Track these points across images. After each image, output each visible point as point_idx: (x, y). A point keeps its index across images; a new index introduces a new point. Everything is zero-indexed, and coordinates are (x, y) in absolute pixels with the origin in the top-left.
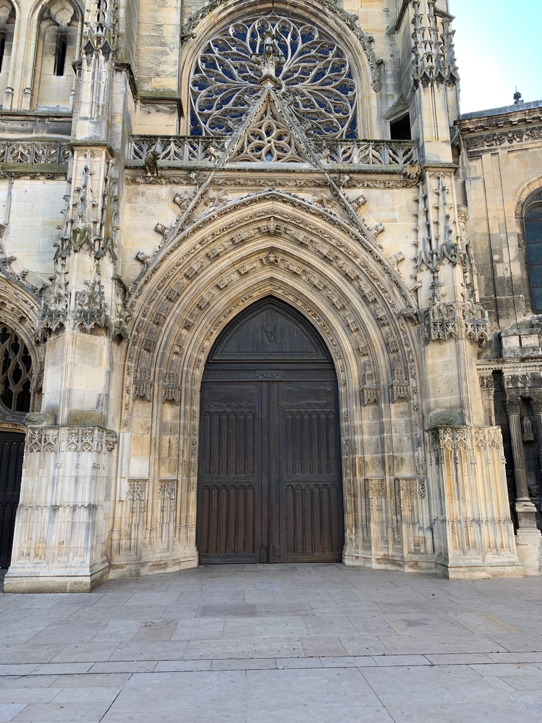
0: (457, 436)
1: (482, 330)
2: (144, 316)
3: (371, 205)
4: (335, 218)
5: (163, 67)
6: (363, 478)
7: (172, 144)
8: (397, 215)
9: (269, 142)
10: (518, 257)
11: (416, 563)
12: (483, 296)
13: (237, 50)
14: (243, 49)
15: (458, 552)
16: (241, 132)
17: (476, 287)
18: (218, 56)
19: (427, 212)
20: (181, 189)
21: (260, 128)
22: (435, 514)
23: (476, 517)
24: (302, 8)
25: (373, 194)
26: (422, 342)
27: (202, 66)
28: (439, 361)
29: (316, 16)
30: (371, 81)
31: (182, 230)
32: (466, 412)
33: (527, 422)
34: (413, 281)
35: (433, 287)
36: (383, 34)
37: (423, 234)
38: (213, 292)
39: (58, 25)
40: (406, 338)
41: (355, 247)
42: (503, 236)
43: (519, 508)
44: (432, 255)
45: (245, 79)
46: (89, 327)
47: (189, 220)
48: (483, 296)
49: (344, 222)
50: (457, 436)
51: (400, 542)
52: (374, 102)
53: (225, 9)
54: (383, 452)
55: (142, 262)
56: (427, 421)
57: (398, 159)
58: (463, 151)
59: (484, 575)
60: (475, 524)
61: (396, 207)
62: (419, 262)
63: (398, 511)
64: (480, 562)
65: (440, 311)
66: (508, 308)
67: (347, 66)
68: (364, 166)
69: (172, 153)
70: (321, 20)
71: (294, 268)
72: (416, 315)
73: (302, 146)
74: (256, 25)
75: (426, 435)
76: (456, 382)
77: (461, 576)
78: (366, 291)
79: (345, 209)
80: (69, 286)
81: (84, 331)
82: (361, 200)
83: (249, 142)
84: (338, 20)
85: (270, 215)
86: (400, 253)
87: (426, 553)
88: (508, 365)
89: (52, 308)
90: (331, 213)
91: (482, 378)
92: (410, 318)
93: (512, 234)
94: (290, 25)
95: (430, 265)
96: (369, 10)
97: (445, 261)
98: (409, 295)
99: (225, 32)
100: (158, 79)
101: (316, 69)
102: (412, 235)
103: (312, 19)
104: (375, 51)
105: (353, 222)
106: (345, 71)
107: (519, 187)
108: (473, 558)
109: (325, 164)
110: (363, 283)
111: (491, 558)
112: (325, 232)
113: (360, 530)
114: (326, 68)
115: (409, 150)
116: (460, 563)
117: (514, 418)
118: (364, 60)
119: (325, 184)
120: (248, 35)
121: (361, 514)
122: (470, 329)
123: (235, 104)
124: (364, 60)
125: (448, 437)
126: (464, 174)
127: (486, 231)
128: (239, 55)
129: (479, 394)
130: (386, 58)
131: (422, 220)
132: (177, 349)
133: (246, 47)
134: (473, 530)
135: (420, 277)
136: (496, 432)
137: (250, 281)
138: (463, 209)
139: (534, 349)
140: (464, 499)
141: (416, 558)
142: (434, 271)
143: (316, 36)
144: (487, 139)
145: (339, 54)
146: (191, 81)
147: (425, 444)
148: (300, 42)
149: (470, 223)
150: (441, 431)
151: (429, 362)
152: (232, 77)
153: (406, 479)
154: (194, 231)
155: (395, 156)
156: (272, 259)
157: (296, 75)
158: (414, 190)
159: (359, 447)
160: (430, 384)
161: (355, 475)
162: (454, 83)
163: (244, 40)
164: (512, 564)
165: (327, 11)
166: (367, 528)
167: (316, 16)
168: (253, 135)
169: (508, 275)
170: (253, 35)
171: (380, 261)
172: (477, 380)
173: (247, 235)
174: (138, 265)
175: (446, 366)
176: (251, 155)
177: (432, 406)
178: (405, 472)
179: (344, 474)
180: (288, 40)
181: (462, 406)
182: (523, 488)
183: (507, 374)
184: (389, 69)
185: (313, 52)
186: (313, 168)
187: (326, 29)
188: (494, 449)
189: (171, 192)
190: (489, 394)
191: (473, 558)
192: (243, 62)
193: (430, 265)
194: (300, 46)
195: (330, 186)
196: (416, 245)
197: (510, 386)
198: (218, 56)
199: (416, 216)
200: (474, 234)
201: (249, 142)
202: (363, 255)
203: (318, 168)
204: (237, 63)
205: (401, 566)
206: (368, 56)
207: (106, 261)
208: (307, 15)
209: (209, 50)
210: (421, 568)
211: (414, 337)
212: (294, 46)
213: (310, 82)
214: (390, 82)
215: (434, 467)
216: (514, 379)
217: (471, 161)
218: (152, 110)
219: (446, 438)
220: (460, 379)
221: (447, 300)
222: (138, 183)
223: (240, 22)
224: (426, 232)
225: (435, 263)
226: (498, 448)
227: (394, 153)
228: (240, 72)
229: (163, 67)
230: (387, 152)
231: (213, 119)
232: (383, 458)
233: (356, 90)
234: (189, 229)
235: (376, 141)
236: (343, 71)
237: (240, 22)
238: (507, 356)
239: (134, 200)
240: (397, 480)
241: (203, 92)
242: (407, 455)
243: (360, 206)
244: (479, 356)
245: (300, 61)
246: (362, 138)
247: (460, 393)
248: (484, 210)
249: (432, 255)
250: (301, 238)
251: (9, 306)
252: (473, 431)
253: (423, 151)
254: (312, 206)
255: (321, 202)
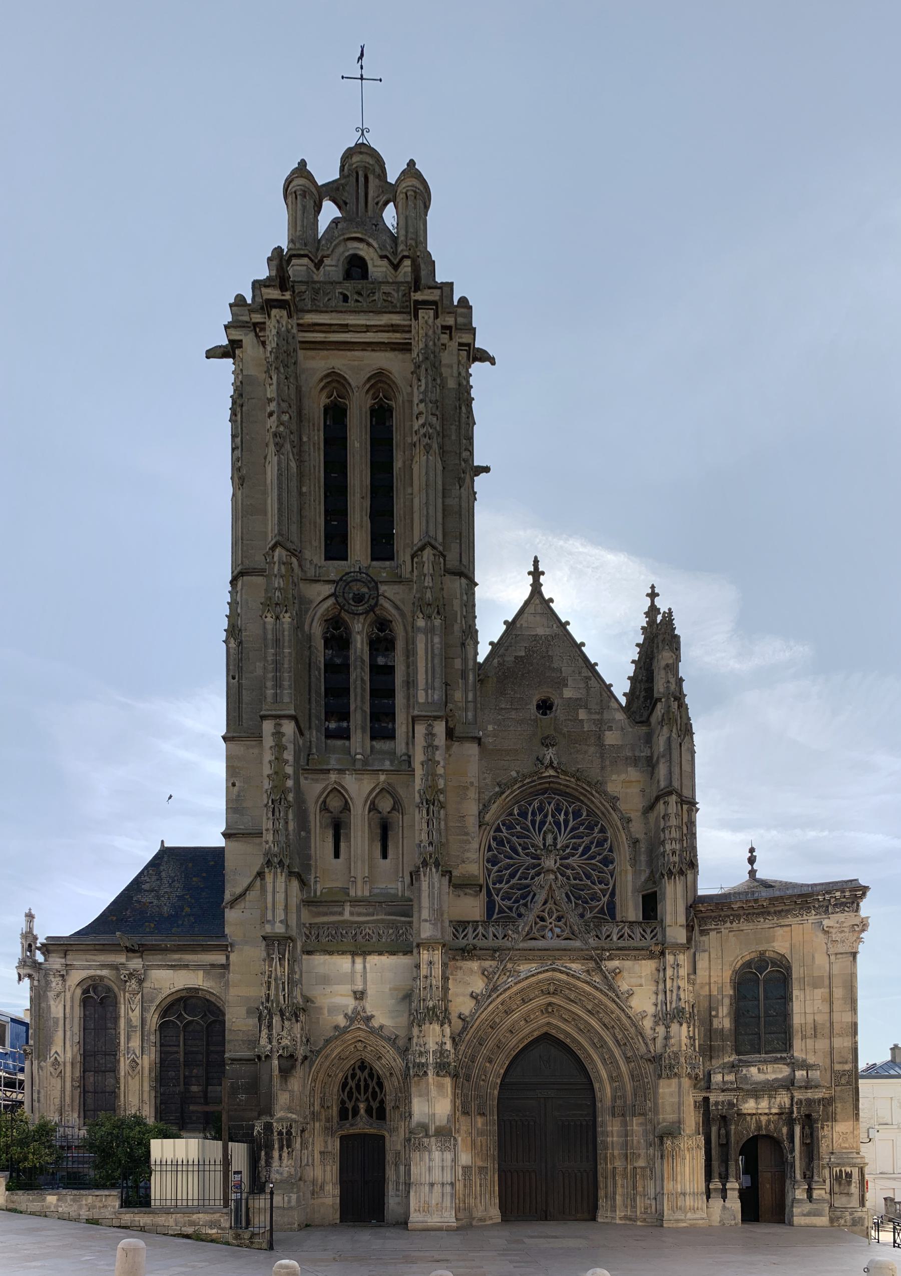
0: (675, 1141)
1: (697, 1071)
2: (466, 1058)
3: (625, 974)
4: (598, 985)
5: (468, 855)
6: (612, 1166)
7: (480, 927)
8: (643, 981)
9: (551, 923)
10: (729, 1013)
11: (645, 1219)
12: (702, 1042)
13: (521, 828)
14: (525, 826)
15: (670, 1212)
16: (531, 917)
17: (697, 1037)
18: (506, 835)
19: (665, 981)
20: (487, 964)
21: (543, 911)
22: (658, 1190)
23: (683, 1191)
24: (573, 788)
25: (628, 964)
26: (657, 1076)
27: (494, 845)
28: (666, 1090)
29: (585, 796)
30: (628, 858)
31: (490, 996)
32: (682, 1126)
33: (723, 1131)
34: (652, 1032)
35: (667, 1038)
36: (639, 814)
37: (661, 997)
38: (507, 1035)
39: (380, 813)
40: (646, 1073)
41: (613, 1006)
42: (720, 997)
43: (711, 1187)
44: (667, 1015)
45: (527, 854)
46: (441, 1074)
47: (495, 989)
48: (702, 1042)
49: (604, 988)
50: (675, 1141)
51: (635, 1207)
52: (630, 877)
53: (512, 793)
54: (627, 1150)
55: (463, 1020)
56: (657, 1130)
57: (646, 936)
58: (696, 928)
59: (684, 1225)
60: (682, 1196)
61: (643, 975)
62: (657, 1018)
63: (635, 1187)
64: (683, 1217)
65: (669, 1056)
66: (718, 1051)
67: (609, 841)
68: (621, 943)
69: (480, 934)
70: (589, 799)
71: (566, 1017)
72: (653, 1057)
73: (576, 928)
74: (536, 804)
75: (656, 1139)
76: (677, 1106)
77: (670, 1226)
78: (619, 1037)
79: (606, 977)
80: (427, 1046)
81: (438, 1075)
82: (618, 971)
83: (536, 923)
84: (603, 801)
85: (551, 981)
86: (644, 1011)
87: (651, 1213)
88: (714, 1094)
89: (418, 1061)
90: (595, 981)
91: (695, 1102)
92: (650, 1060)
93: (726, 995)
94: (563, 804)
95: (665, 1022)
96: (628, 790)
97: (675, 1021)
98: (649, 1042)
99: (511, 814)
100: (464, 865)
101: (584, 844)
102: (654, 996)
103: (581, 798)
104: (632, 830)
105: (611, 988)
106: (607, 846)
107: (734, 960)
108: (679, 1215)
109: (592, 942)
110: (617, 1031)
111: (690, 1216)
112: (591, 994)
113: (609, 1199)
114: (592, 843)
115: (655, 928)
116: (671, 1218)
117: (714, 1129)
118: (623, 837)
119: (591, 958)
120: (530, 815)
121: (610, 1189)
122: (689, 1070)
123: (520, 879)
124: (623, 837)
125: (669, 1142)
126: (696, 946)
127: (708, 993)
128: (522, 833)
129: (692, 1114)
130: (641, 836)
131: (661, 986)
132: (483, 1077)
133: (527, 826)
134: (681, 1198)
135: (657, 1029)
136: (701, 1139)
137: (534, 1026)
138: (692, 977)
139: (732, 1083)
140: (676, 1180)
141: (645, 1216)
142: (667, 1027)
143: (585, 814)
144: (713, 918)
145: (603, 830)
146: (485, 858)
147: (655, 1146)
148: (571, 819)
149: (697, 987)
150: (665, 1139)
151: (661, 1091)
152: (517, 854)
153: (642, 1168)
154: (498, 997)
155: (644, 934)
156: (550, 1010)
157: (568, 851)
158: (656, 961)
159: (610, 1146)
160: (660, 1106)
161: (606, 1164)
162: (693, 868)
163: (526, 819)
164: (703, 1219)
165: (594, 792)
166: (614, 1199)
167: (585, 796)
168: (538, 917)
169: (721, 1027)
170: (534, 814)
171: (630, 1017)
172: (692, 1103)
173: (533, 995)
174: (460, 1021)
175: (671, 1095)
176: (537, 935)
177: (661, 1121)
178: (641, 1163)
179: (599, 1163)
180: (562, 818)
181: (679, 1122)
182: (715, 1174)
183: (712, 1099)
184: (643, 847)
185: (582, 829)
186: (584, 947)
187: (591, 806)
188: (698, 1150)
189: (480, 966)
190: (699, 1113)
191: (679, 1215)
192: (526, 840)
193: (665, 1022)
194: (571, 825)
195: (595, 960)
196: (656, 1005)
197: (714, 1108)
198: (506, 835)
199: (658, 982)
200: (699, 996)
201: (536, 923)
202: (618, 1011)
203: (587, 947)
204: (521, 841)
205: (635, 1221)
206: (626, 835)
207: (446, 1027)
208: (577, 794)
209: (498, 830)
210: (648, 1222)
211: (652, 1074)
212: (566, 822)
213: (580, 856)
214: (643, 858)
215: (660, 1160)
216: (717, 1103)
217: (702, 936)
218: (462, 894)
219: (668, 1143)
220: (680, 1104)
221: (675, 1049)
222: (457, 960)
223: (522, 803)
224: (664, 996)
225: (668, 1021)
226: (701, 1149)
227: (644, 931)
228: (524, 849)
229: (468, 855)
230: (638, 930)
231: (503, 893)
232: (627, 1154)
233: (615, 864)
234: (495, 996)
235: (630, 922)
236: (606, 846)
237: (522, 803)
238: (714, 1087)
239: (455, 973)
240: (635, 1168)
241: (496, 868)
242: (642, 1152)
243: (616, 975)
244: (695, 1087)
245: (571, 838)
246: (620, 920)
247: (679, 1114)
248: (707, 977)
249: (667, 1015)
250: (572, 997)
251: (369, 1048)
252: (686, 1138)
253: (665, 931)
254: (582, 976)
255: (588, 971)
